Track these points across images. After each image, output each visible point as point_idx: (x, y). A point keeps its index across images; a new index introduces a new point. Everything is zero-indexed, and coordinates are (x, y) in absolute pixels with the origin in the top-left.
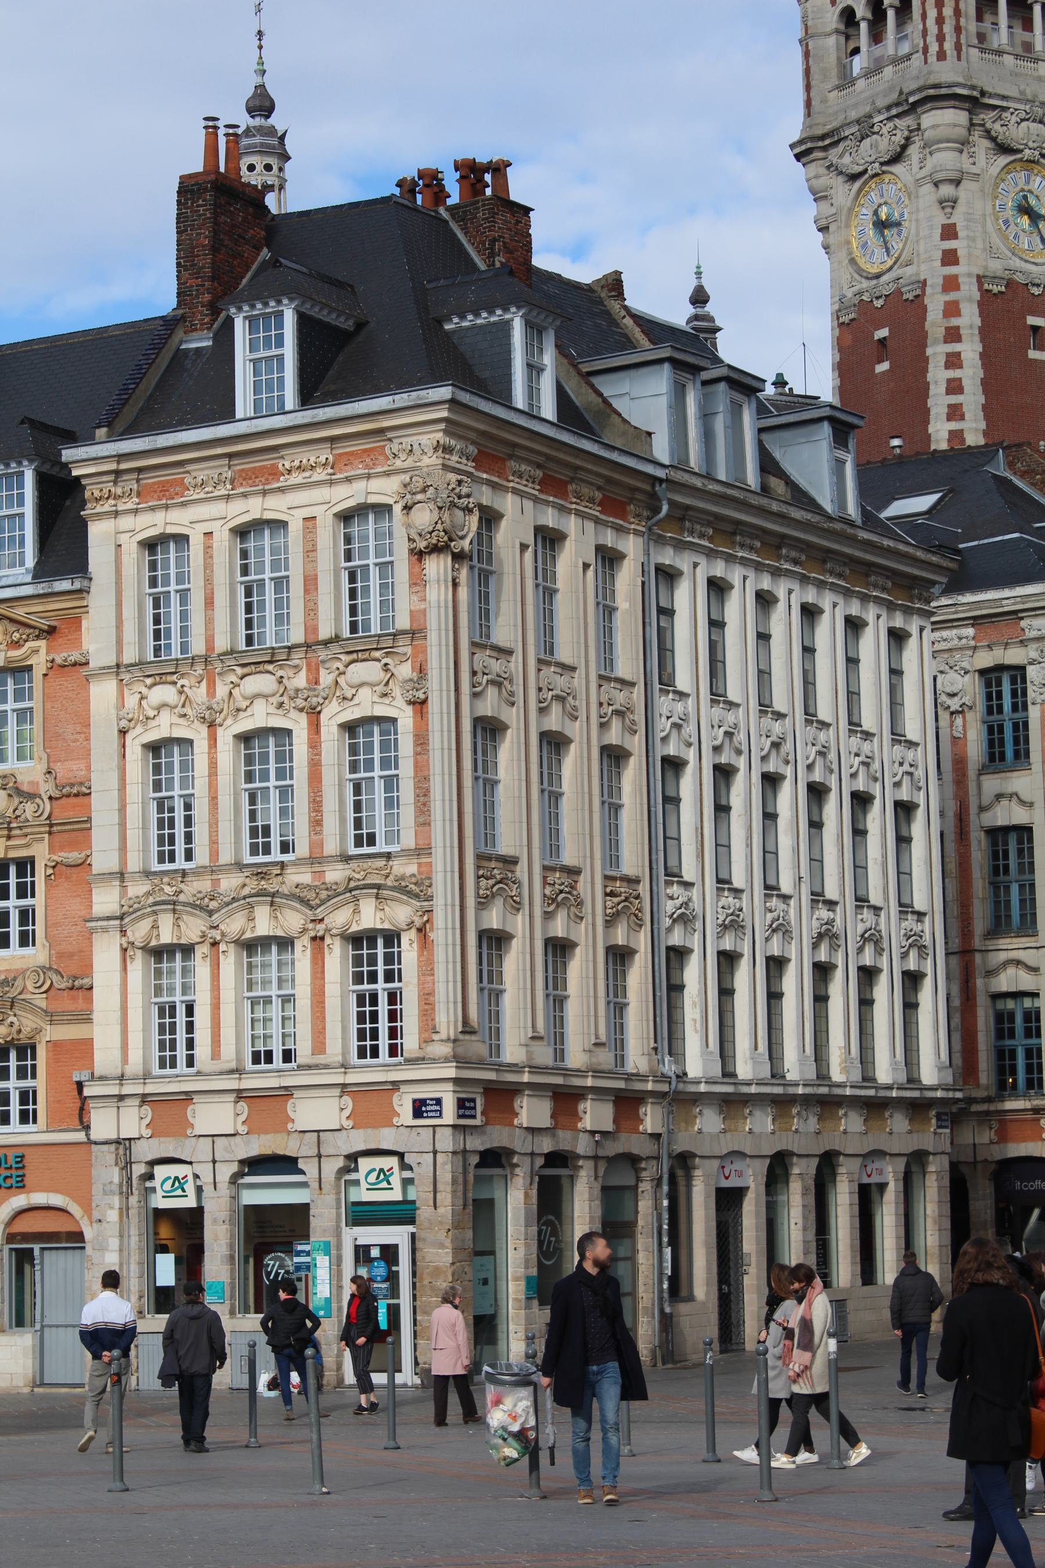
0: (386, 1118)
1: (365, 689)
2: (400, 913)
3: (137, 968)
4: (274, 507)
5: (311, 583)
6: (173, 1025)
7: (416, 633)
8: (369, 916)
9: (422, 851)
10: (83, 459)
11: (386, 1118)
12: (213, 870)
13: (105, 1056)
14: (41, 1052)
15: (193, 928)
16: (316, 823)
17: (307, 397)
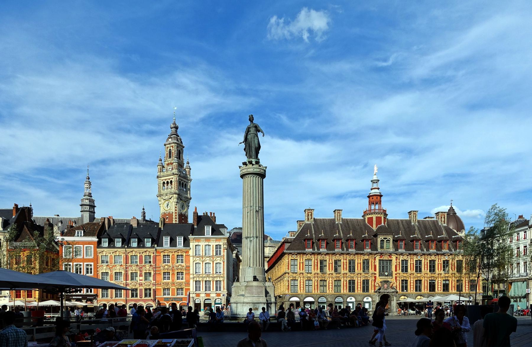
0: (220, 296)
1: (218, 260)
2: (221, 279)
3: (194, 283)
4: (210, 244)
5: (213, 251)
6: (197, 288)
7: (224, 256)
8: (218, 279)
9: (224, 274)
10: (191, 237)
11: (220, 296)
12: (203, 274)
13: (191, 290)
14: (184, 290)
15: (201, 279)
16: (213, 271)
17: (212, 235)
